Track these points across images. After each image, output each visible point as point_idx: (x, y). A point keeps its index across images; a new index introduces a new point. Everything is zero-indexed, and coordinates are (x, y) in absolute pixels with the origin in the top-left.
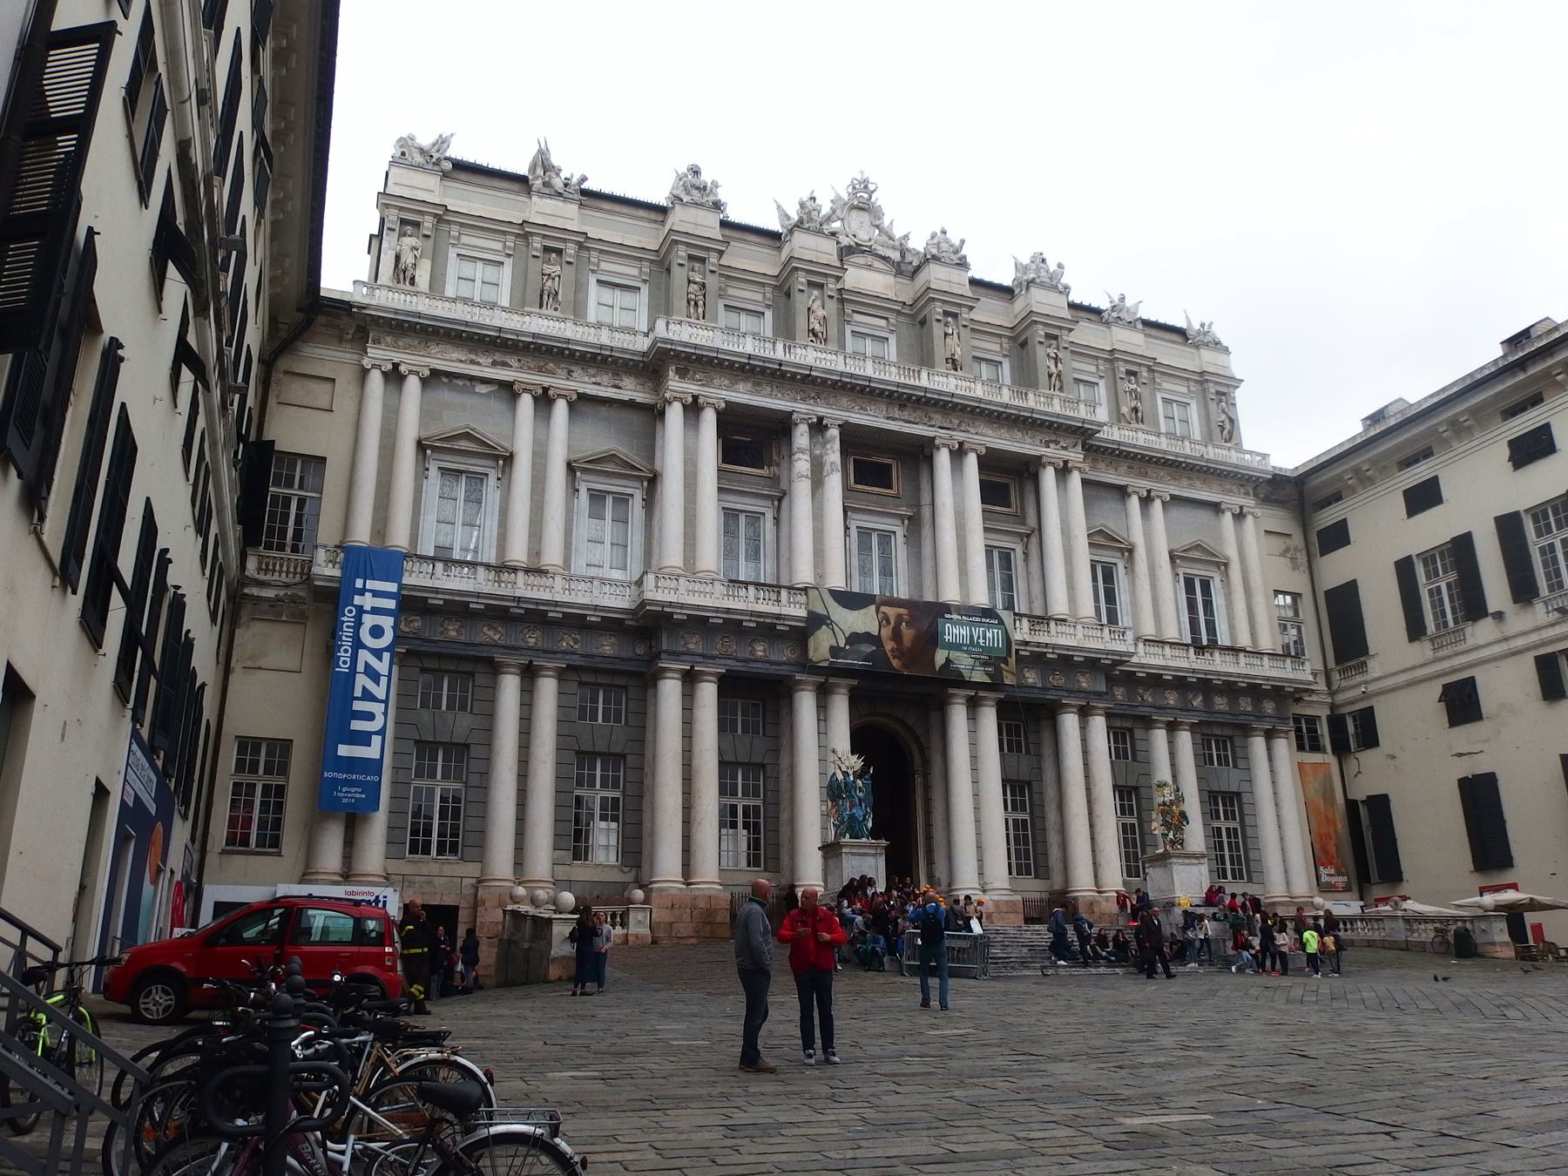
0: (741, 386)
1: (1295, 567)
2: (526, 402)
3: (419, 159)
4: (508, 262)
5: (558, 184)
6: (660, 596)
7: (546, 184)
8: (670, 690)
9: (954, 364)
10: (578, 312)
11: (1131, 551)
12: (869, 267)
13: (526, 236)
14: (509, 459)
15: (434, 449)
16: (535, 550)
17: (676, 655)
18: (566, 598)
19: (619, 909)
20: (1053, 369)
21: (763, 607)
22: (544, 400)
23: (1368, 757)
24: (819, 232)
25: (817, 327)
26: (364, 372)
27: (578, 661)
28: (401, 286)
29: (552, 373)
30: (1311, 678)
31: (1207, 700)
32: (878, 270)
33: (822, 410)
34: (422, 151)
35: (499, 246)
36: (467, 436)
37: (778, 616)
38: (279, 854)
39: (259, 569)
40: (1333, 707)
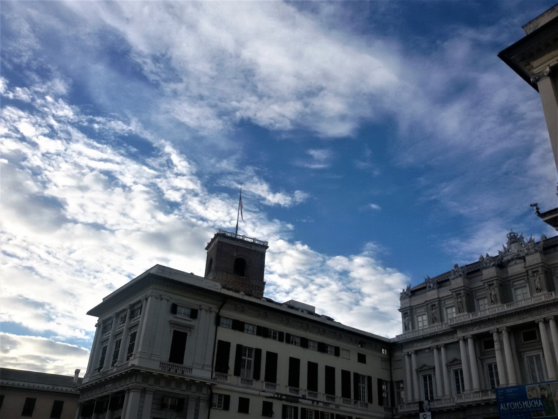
0: (475, 329)
2: (435, 351)
3: (404, 295)
4: (426, 313)
5: (432, 285)
6: (459, 401)
7: (430, 287)
9: (538, 290)
10: (442, 320)
12: (516, 264)
13: (427, 304)
14: (434, 368)
15: (420, 371)
16: (444, 392)
18: (446, 405)
21: (484, 398)
22: (439, 349)
24: (490, 266)
25: (493, 299)
26: (404, 357)
28: (408, 331)
29: (438, 341)
32: (518, 264)
34: (405, 293)
35: (423, 310)
36: (425, 365)
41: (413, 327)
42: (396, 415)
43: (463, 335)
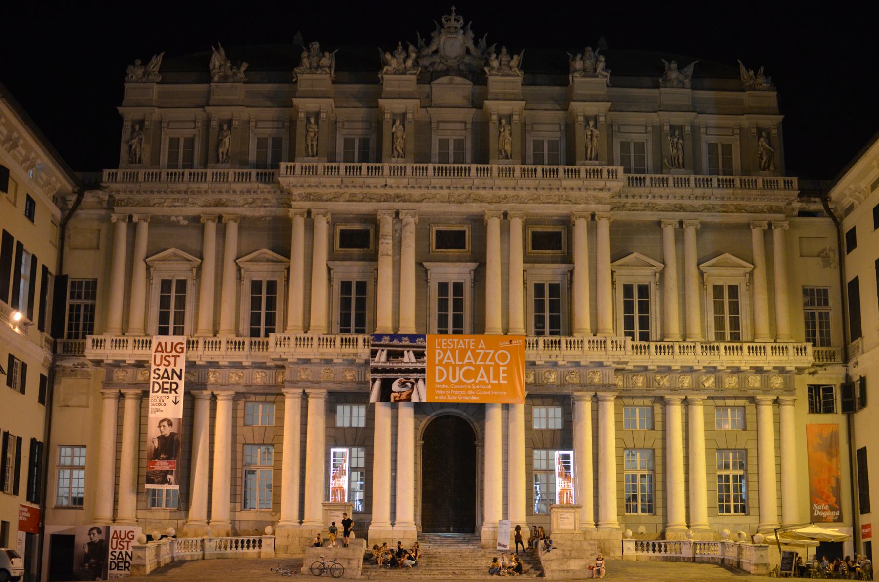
1: (827, 263)
2: (211, 228)
8: (291, 405)
11: (662, 273)
14: (199, 268)
17: (294, 383)
19: (257, 538)
20: (589, 143)
23: (860, 417)
27: (242, 390)
30: (811, 359)
31: (719, 381)
33: (398, 205)
37: (356, 355)
38: (81, 509)
39: (64, 351)
40: (847, 376)
41: (155, 160)
42: (62, 358)
43: (307, 205)
